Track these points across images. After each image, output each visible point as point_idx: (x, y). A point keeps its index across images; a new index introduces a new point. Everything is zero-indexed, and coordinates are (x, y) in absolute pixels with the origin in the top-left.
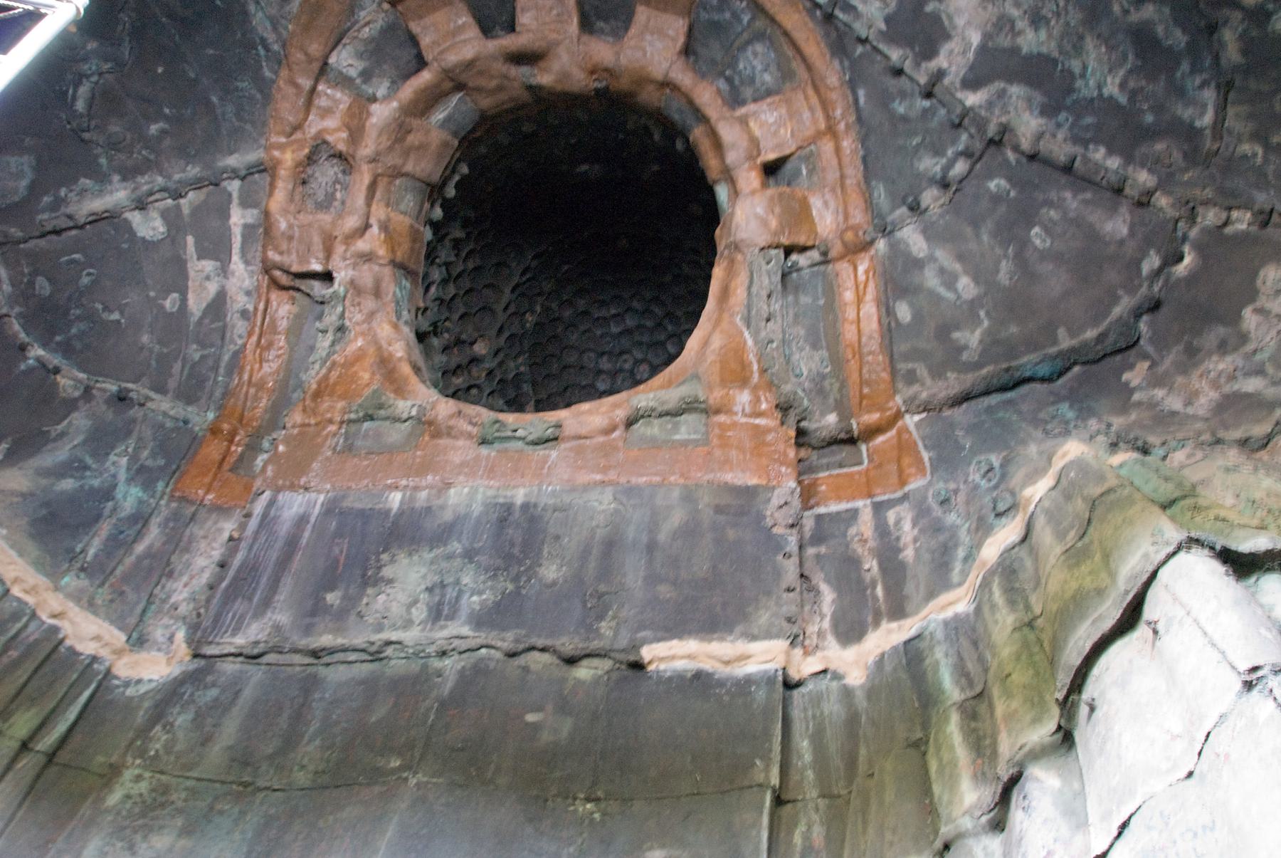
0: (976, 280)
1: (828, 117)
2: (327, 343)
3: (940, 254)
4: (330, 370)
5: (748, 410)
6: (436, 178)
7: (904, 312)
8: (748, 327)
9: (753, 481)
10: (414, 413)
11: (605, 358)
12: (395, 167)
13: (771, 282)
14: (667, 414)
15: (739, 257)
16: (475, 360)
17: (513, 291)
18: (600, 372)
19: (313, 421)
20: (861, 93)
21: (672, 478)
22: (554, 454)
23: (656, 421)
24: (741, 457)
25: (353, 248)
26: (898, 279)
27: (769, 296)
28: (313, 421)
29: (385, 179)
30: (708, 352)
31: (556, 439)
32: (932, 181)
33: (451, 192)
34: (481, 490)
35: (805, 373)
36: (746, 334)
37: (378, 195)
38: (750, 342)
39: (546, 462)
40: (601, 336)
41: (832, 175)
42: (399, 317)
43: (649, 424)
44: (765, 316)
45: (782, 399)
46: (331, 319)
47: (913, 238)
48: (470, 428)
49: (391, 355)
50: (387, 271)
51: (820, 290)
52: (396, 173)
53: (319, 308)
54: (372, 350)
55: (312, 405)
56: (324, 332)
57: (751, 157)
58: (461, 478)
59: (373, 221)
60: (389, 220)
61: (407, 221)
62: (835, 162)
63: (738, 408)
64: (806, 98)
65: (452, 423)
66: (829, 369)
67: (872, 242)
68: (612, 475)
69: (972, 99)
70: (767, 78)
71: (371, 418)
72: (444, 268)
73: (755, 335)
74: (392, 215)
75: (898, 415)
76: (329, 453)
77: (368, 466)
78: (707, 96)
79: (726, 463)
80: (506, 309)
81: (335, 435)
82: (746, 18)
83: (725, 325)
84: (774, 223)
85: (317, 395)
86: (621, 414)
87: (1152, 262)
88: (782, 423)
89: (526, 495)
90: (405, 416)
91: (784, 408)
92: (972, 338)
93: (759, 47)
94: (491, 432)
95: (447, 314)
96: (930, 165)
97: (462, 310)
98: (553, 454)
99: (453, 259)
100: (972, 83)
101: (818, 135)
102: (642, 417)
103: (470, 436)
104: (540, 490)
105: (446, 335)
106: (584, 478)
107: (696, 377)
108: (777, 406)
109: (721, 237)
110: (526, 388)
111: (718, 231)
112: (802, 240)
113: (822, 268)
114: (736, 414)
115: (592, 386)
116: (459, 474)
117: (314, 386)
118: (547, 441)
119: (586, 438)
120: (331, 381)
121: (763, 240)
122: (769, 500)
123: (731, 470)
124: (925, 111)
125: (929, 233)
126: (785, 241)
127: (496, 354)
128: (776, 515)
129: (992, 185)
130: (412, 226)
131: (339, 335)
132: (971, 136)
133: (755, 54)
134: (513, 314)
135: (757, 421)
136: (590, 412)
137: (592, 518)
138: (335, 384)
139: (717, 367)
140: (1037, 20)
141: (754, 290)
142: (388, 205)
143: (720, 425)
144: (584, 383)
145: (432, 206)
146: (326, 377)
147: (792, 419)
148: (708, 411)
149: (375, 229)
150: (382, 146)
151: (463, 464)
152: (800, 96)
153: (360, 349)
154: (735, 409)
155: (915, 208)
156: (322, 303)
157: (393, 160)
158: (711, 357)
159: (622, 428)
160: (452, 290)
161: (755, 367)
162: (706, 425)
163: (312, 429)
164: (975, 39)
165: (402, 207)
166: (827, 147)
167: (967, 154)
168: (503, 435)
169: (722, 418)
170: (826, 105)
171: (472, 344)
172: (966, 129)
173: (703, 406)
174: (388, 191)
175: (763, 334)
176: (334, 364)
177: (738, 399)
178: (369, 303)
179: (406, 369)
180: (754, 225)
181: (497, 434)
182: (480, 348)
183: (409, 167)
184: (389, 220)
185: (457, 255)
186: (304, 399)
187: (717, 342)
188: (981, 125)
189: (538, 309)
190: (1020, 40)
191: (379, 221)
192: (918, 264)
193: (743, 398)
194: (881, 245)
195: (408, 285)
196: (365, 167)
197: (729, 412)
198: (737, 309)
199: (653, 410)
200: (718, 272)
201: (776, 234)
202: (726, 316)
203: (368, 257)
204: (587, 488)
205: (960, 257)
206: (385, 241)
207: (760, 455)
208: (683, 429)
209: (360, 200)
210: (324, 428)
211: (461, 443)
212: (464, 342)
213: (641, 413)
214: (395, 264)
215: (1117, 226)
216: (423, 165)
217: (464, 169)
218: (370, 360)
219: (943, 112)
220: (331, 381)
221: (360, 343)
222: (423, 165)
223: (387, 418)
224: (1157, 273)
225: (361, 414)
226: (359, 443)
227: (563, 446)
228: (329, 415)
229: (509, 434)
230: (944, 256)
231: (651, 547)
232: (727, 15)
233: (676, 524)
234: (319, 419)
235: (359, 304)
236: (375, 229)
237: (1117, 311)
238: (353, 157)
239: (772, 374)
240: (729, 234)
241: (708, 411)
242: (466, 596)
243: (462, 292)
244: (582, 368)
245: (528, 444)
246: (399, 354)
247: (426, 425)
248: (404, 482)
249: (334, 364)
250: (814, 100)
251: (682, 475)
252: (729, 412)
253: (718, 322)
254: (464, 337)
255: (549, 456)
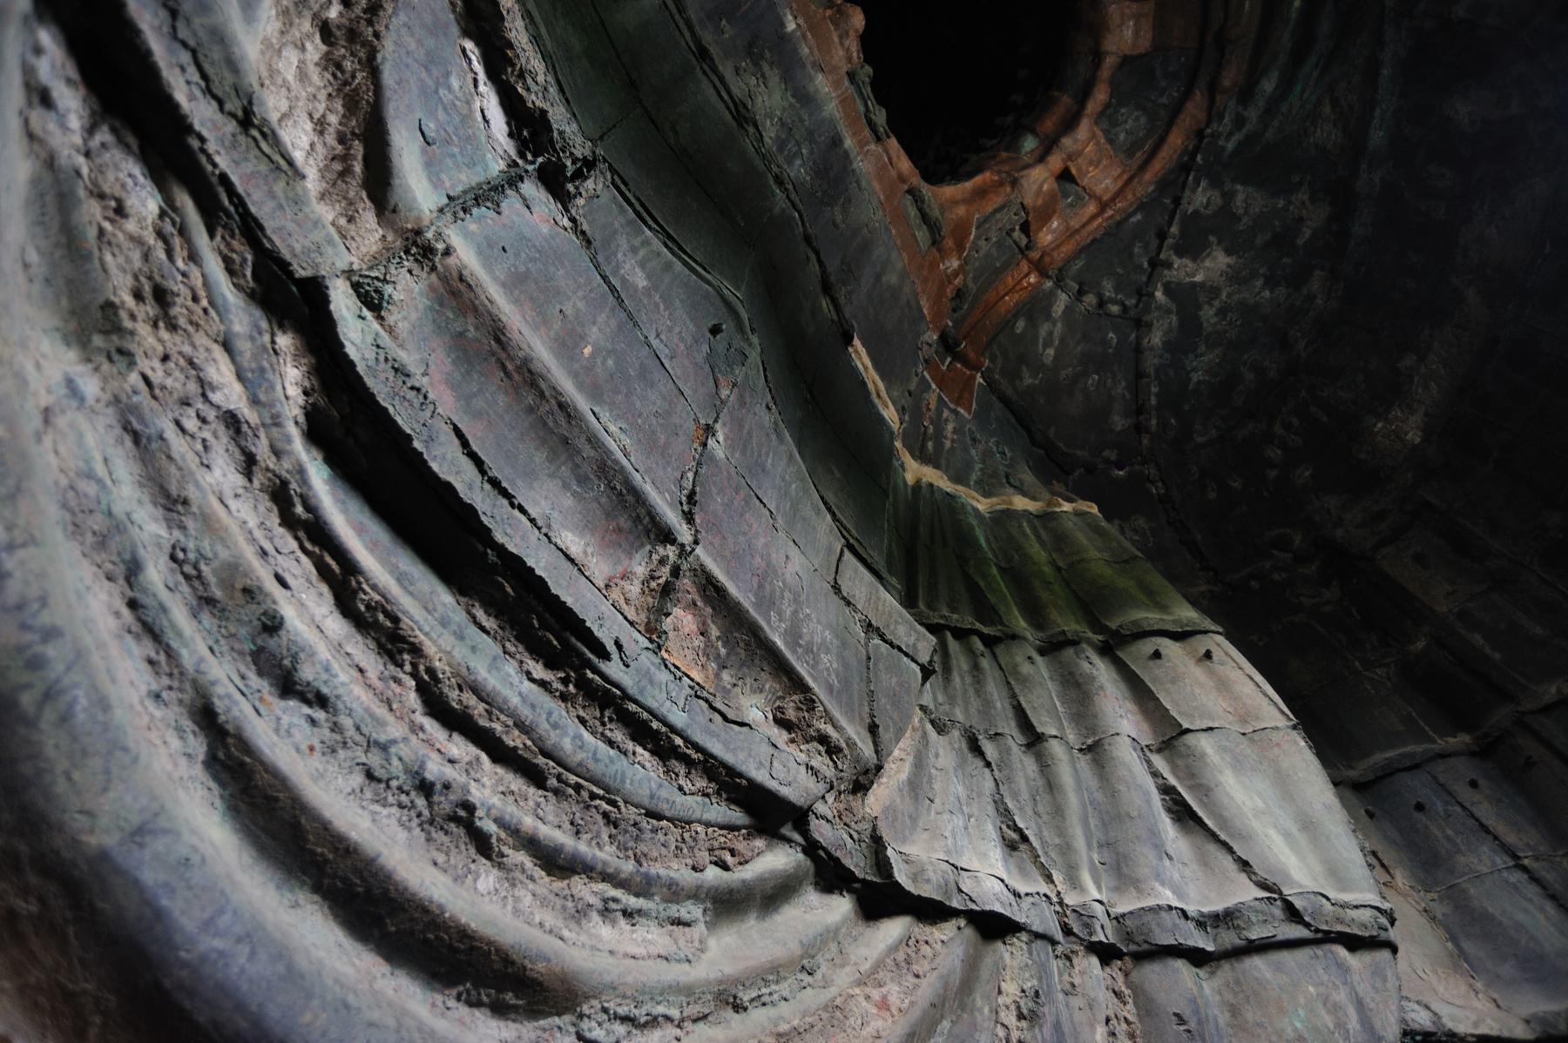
0: (1055, 358)
1: (1113, 199)
3: (1059, 325)
7: (1020, 325)
9: (925, 311)
20: (1139, 217)
26: (1036, 307)
32: (1100, 296)
41: (1075, 223)
47: (1062, 301)
57: (1070, 157)
62: (1084, 220)
64: (1120, 176)
67: (1049, 277)
69: (1159, 294)
70: (1122, 136)
75: (977, 368)
78: (1100, 96)
82: (1164, 100)
87: (1111, 455)
92: (1028, 381)
93: (1143, 120)
96: (1108, 288)
100: (1168, 290)
101: (1099, 199)
103: (849, 59)
121: (1028, 201)
124: (1141, 266)
125: (1068, 309)
129: (1111, 335)
132: (1136, 306)
133: (1137, 119)
140: (1222, 312)
141: (998, 216)
152: (1119, 171)
155: (1081, 293)
159: (906, 187)
164: (1199, 278)
166: (1092, 208)
167: (1125, 308)
170: (1119, 193)
172: (1139, 301)
188: (1147, 310)
190: (1206, 307)
192: (1048, 317)
194: (1049, 284)
199: (923, 201)
205: (1062, 340)
215: (1119, 422)
219: (1144, 279)
224: (1107, 461)
230: (1059, 329)
231: (878, 277)
232: (1163, 84)
237: (1079, 453)
242: (799, 162)
250: (1120, 184)
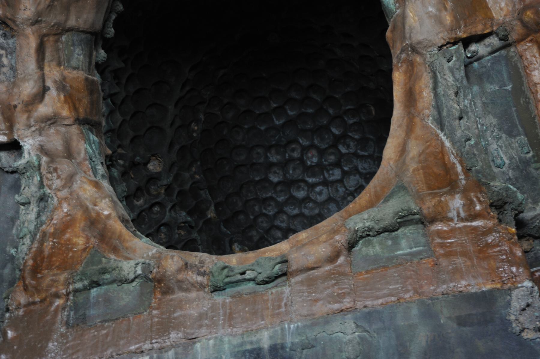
2: (32, 216)
4: (42, 243)
5: (463, 214)
6: (98, 26)
8: (442, 130)
9: (487, 287)
10: (139, 272)
11: (273, 151)
12: (57, 25)
13: (456, 80)
14: (386, 230)
15: (418, 59)
16: (153, 178)
17: (176, 105)
18: (272, 164)
19: (37, 299)
21: (407, 296)
22: (287, 290)
23: (375, 240)
24: (469, 263)
25: (35, 114)
27: (457, 94)
28: (37, 299)
29: (51, 38)
30: (408, 160)
31: (284, 274)
33: (111, 32)
34: (226, 339)
35: (507, 162)
36: (441, 135)
37: (48, 55)
38: (448, 144)
39: (281, 300)
40: (267, 130)
42: (95, 173)
43: (369, 243)
44: (457, 114)
45: (495, 198)
46: (30, 189)
48: (200, 278)
49: (98, 214)
50: (74, 130)
51: (505, 75)
52: (61, 30)
53: (11, 178)
54: (79, 214)
55: (33, 282)
56: (27, 204)
58: (204, 330)
59: (49, 83)
60: (64, 78)
61: (81, 75)
63: (453, 214)
65: (180, 277)
66: (530, 155)
68: (347, 303)
71: (97, 284)
72: (109, 101)
73: (451, 136)
74: (66, 72)
76: (63, 330)
77: (107, 335)
79: (456, 273)
80: (172, 124)
81: (64, 309)
83: (418, 131)
84: (448, 19)
85: (36, 270)
86: (341, 239)
88: (500, 221)
89: (271, 337)
90: (132, 276)
91: (498, 205)
94: (220, 279)
95: (118, 142)
97: (131, 134)
98: (285, 290)
99: (117, 90)
102: (361, 237)
103: (202, 287)
104: (283, 329)
105: (121, 162)
106: (322, 309)
107: (402, 188)
108: (491, 205)
109: (394, 41)
110: (204, 194)
111: (388, 34)
112: (479, 29)
113: (503, 52)
114: (451, 220)
115: (266, 180)
116: (201, 326)
117: (30, 262)
118: (277, 277)
119: (313, 268)
120: (46, 252)
122: (509, 304)
123: (462, 278)
126: (461, 34)
127: (170, 170)
128: (521, 319)
130: (87, 79)
131: (42, 204)
134: (180, 127)
135: (475, 224)
136: (311, 243)
137: (341, 352)
138: (51, 256)
139: (420, 176)
141: (440, 90)
142: (59, 64)
143: (439, 233)
144: (257, 179)
145: (97, 51)
146: (40, 251)
147: (509, 215)
148: (425, 221)
149: (53, 92)
150: (41, 7)
151: (201, 316)
153: (67, 214)
154: (450, 215)
156: (13, 172)
157: (53, 19)
158: (412, 166)
159: (345, 252)
160: (119, 118)
161: (459, 168)
162: (424, 235)
163: (37, 306)
165: (74, 63)
168: (233, 279)
169: (439, 226)
171: (146, 164)
173: (417, 216)
174: (57, 50)
175: (459, 133)
176: (44, 234)
177: (451, 205)
178: (65, 167)
179: (118, 226)
180: (428, 23)
181: (227, 280)
182: (154, 166)
183: (72, 22)
184: (64, 78)
185: (117, 84)
186: (23, 278)
187: (414, 149)
189: (202, 117)
191: (55, 82)
193: (457, 203)
195: (96, 139)
196: (29, 31)
197: (447, 219)
198: (427, 112)
199: (370, 229)
200: (398, 77)
201: (452, 29)
202: (417, 120)
203: (52, 120)
204: (327, 319)
206: (66, 101)
207: (486, 258)
208: (404, 243)
209: (32, 65)
210: (51, 304)
211: (193, 295)
212: (139, 164)
213: (359, 234)
214: (80, 122)
216: (85, 16)
217: (120, 7)
218: (80, 224)
220: (46, 252)
221: (66, 209)
222: (85, 16)
223: (113, 282)
225: (86, 283)
226: (92, 312)
227: (293, 280)
228: (54, 290)
229: (240, 277)
233: (424, 343)
234: (44, 295)
235: (56, 170)
236: (53, 92)
238: (14, 22)
239: (478, 172)
240: (404, 38)
241: (425, 221)
243: (128, 118)
244: (254, 164)
245: (258, 284)
246: (106, 213)
247: (156, 283)
248: (147, 346)
249: (44, 234)
251: (416, 291)
252: (447, 219)
253: (410, 130)
254: (138, 159)
255: (282, 293)
